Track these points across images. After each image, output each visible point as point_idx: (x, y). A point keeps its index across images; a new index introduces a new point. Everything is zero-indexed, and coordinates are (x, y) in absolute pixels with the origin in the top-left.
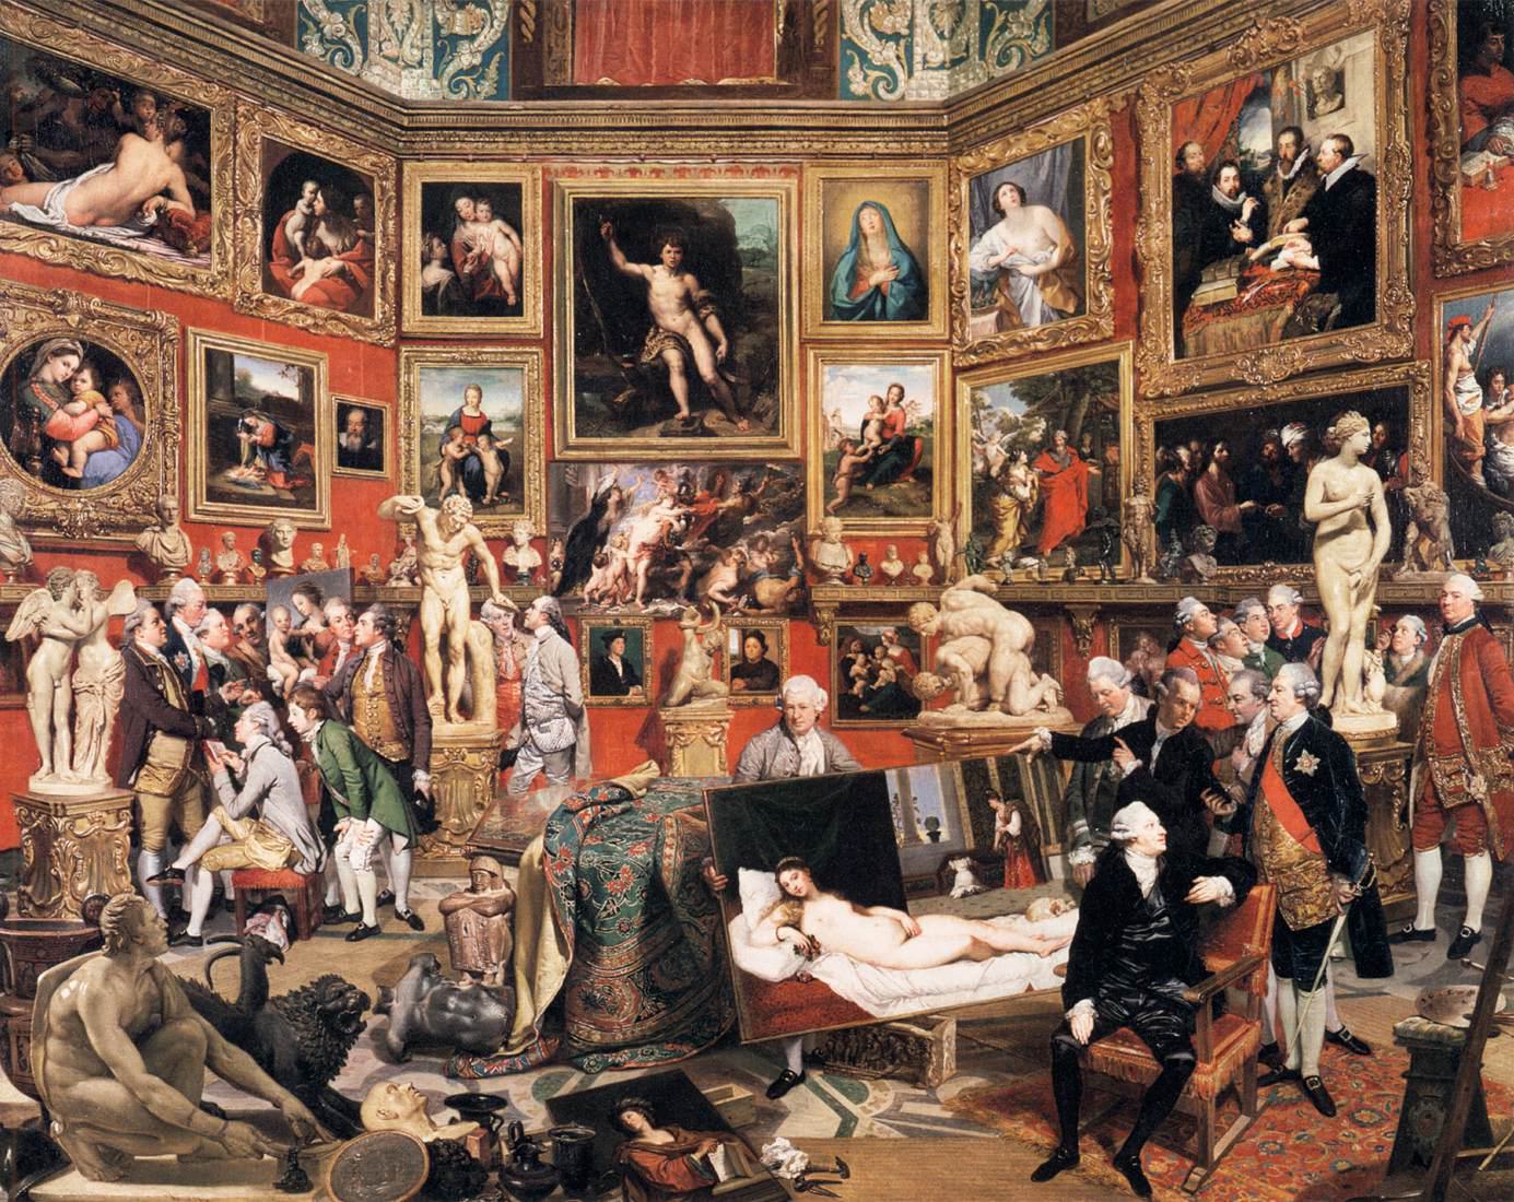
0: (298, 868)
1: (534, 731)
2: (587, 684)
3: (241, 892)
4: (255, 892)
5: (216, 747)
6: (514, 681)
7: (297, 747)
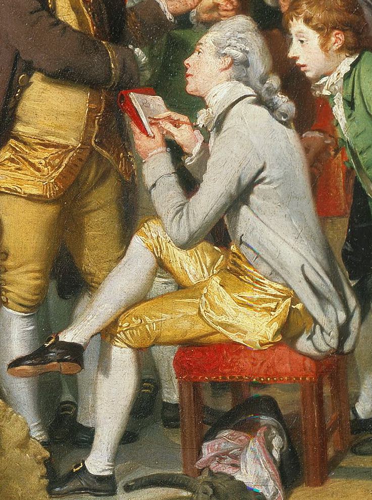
0: (304, 344)
3: (191, 387)
4: (218, 387)
5: (149, 105)
7: (305, 106)
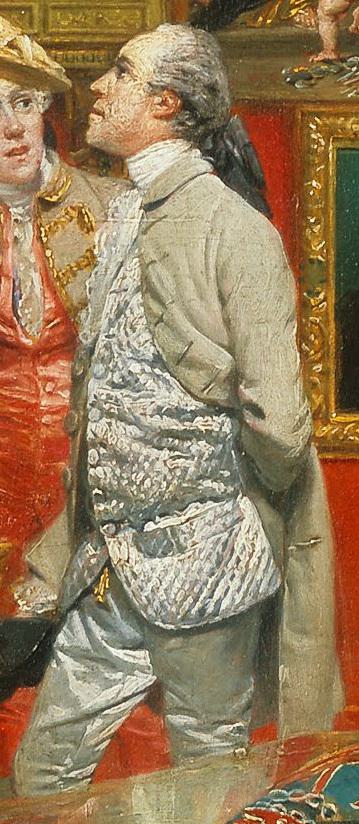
1: (121, 548)
2: (327, 366)
6: (46, 352)
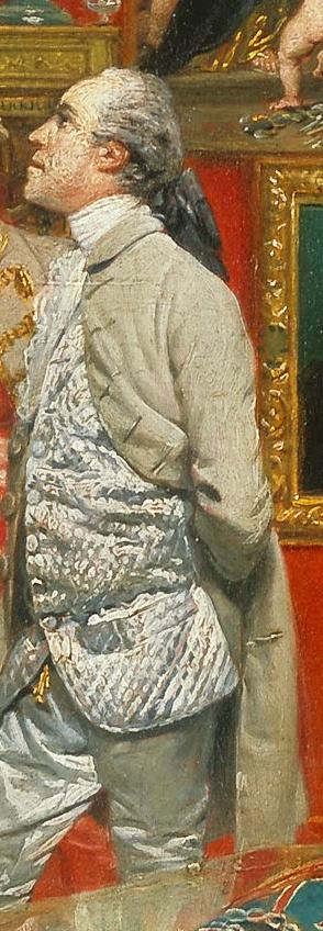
1: (63, 644)
2: (289, 444)
